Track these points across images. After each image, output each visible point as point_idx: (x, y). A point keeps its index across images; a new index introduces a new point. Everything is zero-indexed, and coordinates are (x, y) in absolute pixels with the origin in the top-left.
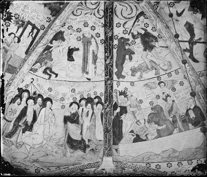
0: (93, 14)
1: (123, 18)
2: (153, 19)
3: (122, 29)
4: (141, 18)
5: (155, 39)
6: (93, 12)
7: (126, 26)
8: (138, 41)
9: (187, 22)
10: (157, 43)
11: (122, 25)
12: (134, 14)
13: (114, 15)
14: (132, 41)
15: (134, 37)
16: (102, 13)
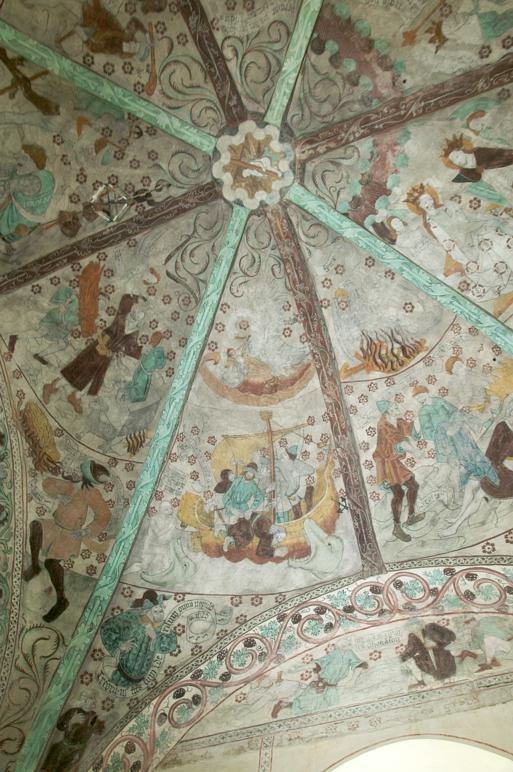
0: (245, 39)
1: (180, 59)
2: (126, 100)
3: (172, 33)
4: (145, 79)
5: (93, 44)
6: (245, 44)
7: (165, 44)
8: (124, 20)
9: (59, 114)
10: (85, 38)
11: (176, 43)
12: (165, 76)
13: (202, 62)
14: (135, 11)
15: (138, 25)
16: (228, 53)
